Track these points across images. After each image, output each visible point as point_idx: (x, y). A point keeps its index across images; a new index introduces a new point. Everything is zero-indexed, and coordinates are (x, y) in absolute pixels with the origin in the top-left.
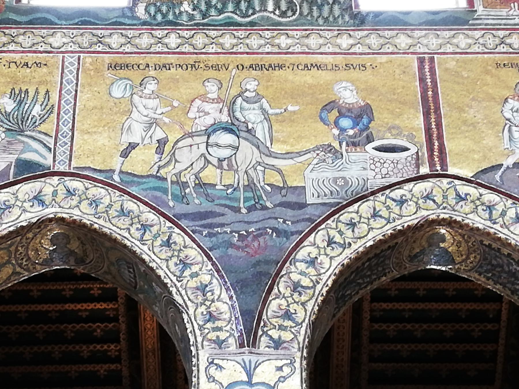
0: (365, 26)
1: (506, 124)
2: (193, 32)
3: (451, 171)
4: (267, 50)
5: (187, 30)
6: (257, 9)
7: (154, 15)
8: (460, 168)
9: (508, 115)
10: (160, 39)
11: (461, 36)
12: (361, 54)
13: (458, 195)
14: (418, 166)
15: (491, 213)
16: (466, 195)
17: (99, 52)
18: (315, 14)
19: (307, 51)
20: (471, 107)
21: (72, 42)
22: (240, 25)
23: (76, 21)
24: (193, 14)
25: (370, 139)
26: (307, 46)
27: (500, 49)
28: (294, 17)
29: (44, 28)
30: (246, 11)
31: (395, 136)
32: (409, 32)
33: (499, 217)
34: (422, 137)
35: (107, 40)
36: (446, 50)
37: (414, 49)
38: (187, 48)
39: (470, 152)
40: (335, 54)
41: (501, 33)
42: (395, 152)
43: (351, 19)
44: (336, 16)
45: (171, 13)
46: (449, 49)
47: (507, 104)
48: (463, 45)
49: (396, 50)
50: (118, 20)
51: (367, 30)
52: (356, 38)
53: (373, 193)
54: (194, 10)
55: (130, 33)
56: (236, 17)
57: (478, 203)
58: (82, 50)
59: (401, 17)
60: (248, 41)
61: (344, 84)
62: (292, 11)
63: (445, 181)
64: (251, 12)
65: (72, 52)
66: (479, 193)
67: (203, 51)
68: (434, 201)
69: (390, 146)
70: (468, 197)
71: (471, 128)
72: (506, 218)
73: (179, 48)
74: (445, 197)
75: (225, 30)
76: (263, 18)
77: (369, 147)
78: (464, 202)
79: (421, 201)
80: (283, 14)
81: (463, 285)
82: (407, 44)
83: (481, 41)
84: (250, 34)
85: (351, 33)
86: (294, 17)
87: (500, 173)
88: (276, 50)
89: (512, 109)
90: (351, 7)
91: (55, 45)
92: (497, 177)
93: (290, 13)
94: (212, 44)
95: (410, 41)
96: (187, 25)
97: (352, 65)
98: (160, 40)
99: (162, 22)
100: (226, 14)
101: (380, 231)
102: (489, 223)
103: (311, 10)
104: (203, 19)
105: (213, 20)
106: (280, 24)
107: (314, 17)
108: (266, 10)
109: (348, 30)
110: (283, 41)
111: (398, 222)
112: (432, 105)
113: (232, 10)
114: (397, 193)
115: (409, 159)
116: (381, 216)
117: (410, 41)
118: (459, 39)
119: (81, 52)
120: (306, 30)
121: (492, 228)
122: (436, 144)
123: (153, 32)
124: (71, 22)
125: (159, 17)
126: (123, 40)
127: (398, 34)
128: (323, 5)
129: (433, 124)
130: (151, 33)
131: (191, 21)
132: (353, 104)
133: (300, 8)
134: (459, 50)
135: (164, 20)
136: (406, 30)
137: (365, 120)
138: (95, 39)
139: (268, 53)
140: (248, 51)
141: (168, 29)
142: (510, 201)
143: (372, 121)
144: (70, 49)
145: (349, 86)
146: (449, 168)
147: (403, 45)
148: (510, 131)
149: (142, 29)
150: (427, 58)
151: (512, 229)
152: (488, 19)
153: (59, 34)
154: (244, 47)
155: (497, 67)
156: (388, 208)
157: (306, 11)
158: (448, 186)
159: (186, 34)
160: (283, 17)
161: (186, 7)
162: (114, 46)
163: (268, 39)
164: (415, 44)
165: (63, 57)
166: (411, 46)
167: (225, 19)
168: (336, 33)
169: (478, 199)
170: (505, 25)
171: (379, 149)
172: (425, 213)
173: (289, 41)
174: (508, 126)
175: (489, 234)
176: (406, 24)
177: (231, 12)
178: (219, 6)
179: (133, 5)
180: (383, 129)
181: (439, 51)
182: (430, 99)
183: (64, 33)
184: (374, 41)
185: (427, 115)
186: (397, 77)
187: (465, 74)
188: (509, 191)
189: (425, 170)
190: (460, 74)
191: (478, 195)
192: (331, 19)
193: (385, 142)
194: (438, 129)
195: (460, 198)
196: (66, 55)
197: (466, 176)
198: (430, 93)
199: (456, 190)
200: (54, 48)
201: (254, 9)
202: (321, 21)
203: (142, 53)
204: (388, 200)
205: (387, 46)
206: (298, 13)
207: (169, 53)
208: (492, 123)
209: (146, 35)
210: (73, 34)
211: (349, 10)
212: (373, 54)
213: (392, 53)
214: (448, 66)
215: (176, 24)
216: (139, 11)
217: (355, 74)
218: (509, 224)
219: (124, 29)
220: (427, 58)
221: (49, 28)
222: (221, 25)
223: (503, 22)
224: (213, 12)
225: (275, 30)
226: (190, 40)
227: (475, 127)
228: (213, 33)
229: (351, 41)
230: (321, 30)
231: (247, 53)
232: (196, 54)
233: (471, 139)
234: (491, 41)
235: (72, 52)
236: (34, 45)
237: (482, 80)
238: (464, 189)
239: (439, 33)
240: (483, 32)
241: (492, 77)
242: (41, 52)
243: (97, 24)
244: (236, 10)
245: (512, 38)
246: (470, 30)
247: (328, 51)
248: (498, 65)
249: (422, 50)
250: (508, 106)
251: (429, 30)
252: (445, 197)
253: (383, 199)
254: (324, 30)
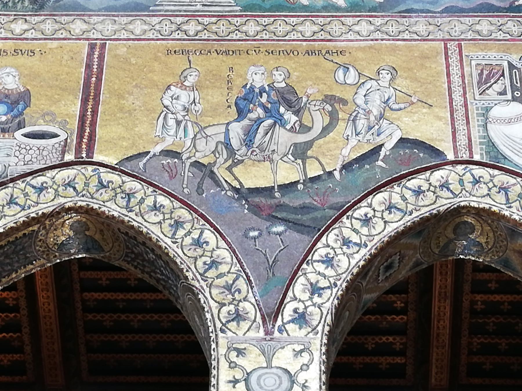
0: (43, 11)
1: (163, 111)
3: (97, 157)
8: (106, 156)
9: (167, 102)
11: (138, 22)
13: (100, 182)
14: (63, 153)
15: (129, 201)
16: (109, 182)
20: (131, 94)
25: (20, 126)
27: (175, 35)
31: (47, 123)
32: (86, 18)
33: (136, 205)
34: (75, 124)
36: (120, 36)
37: (88, 35)
39: (119, 139)
40: (6, 39)
41: (179, 20)
42: (44, 139)
43: (31, 5)
46: (124, 35)
47: (169, 91)
48: (138, 32)
49: (69, 36)
51: (45, 15)
52: (32, 23)
53: (13, 180)
57: (119, 190)
61: (8, 70)
63: (90, 168)
66: (122, 180)
68: (74, 188)
69: (39, 133)
70: (110, 184)
71: (127, 114)
72: (144, 206)
74: (87, 185)
77: (18, 134)
78: (105, 189)
79: (60, 189)
81: (114, 275)
82: (81, 30)
83: (157, 27)
85: (28, 18)
87: (145, 161)
89: (172, 97)
92: (141, 165)
95: (85, 27)
97: (21, 51)
101: (12, 218)
102: (124, 211)
109: (25, 15)
111: (33, 209)
112: (92, 91)
114: (38, 181)
115: (57, 146)
116: (16, 204)
117: (85, 27)
118: (136, 26)
121: (127, 216)
122: (88, 130)
127: (75, 19)
129: (90, 110)
132: (12, 90)
134: (132, 37)
137: (20, 107)
142: (151, 189)
143: (28, 106)
145: (13, 72)
146: (95, 155)
147: (77, 31)
148: (165, 118)
150: (98, 44)
151: (146, 217)
152: (170, 5)
155: (168, 54)
156: (26, 195)
158: (92, 174)
164: (89, 30)
166: (84, 32)
168: (12, 17)
169: (120, 187)
170: (185, 11)
171: (27, 136)
172: (62, 200)
174: (164, 113)
175: (123, 222)
176: (85, 9)
180: (38, 116)
181: (113, 37)
182: (93, 85)
184: (49, 26)
185: (85, 101)
186: (64, 62)
187: (133, 61)
188: (150, 179)
189: (69, 157)
190: (128, 60)
191: (121, 182)
193: (36, 128)
194: (93, 116)
195: (102, 185)
197: (111, 163)
198: (94, 79)
199: (99, 177)
204: (28, 187)
205: (61, 32)
208: (148, 111)
212: (45, 39)
213: (64, 39)
214: (118, 52)
217: (21, 60)
218: (145, 212)
220: (98, 44)
223: (184, 8)
227: (130, 114)
229: (26, 26)
233: (123, 126)
234: (167, 27)
237: (150, 66)
238: (107, 176)
239: (116, 18)
240: (162, 18)
241: (160, 64)
245: (189, 25)
248: (169, 52)
250: (170, 93)
251: (107, 15)
252: (87, 185)
253: (23, 186)
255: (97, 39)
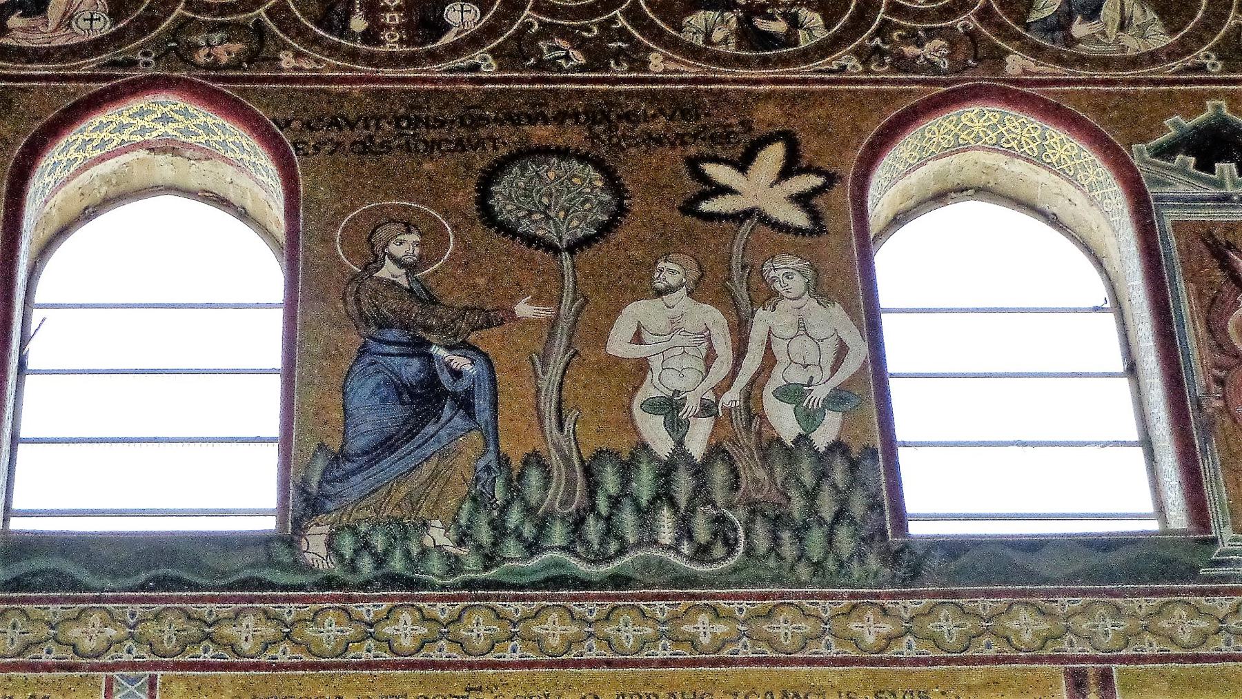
0: (923, 585)
2: (461, 604)
4: (661, 654)
5: (441, 599)
6: (631, 538)
7: (353, 561)
10: (371, 626)
11: (1180, 611)
12: (917, 662)
17: (206, 666)
18: (788, 551)
19: (770, 654)
21: (132, 636)
22: (586, 584)
23: (143, 577)
24: (456, 557)
26: (769, 642)
28: (732, 562)
29: (54, 601)
30: (601, 545)
32: (1039, 601)
35: (227, 630)
38: (443, 651)
40: (845, 662)
43: (886, 566)
44: (845, 557)
45: (398, 554)
50: (256, 573)
52: (902, 618)
54: (460, 543)
55: (289, 611)
56: (573, 561)
58: (158, 659)
59: (1017, 557)
60: (608, 630)
62: (726, 542)
64: (613, 547)
65: (133, 666)
67: (490, 657)
73: (423, 652)
75: (545, 598)
76: (647, 565)
80: (702, 553)
82: (1035, 634)
84: (614, 608)
85: (888, 603)
86: (732, 562)
88: (686, 653)
90: (883, 533)
91: (87, 645)
93: (719, 550)
94: (511, 639)
96: (443, 587)
98: (370, 630)
99: (376, 579)
100: (547, 555)
103: (776, 539)
104: (486, 568)
105: (511, 572)
106: (692, 580)
107: (782, 559)
108: (656, 542)
109: (878, 596)
110: (705, 629)
113: (564, 544)
117: (1044, 626)
119: (156, 666)
120: (765, 597)
123: (351, 606)
124: (129, 582)
125: (366, 565)
126: (269, 631)
128: (806, 527)
130: (345, 610)
131: (454, 575)
133: (747, 537)
134: (1175, 651)
135: (380, 573)
136: (1031, 594)
138: (193, 630)
139: (664, 663)
140: (610, 656)
141: (391, 599)
144: (126, 658)
147: (1027, 637)
149: (322, 599)
153: (96, 618)
154: (601, 648)
157: (762, 544)
159: (442, 611)
160: (702, 562)
161: (438, 536)
162: (246, 647)
163: (664, 623)
164: (1056, 632)
165: (110, 681)
167: (547, 567)
173: (721, 628)
176: (1032, 577)
177: (562, 549)
178: (528, 531)
179: (294, 533)
183: (110, 613)
184: (947, 625)
192: (831, 566)
196: (115, 674)
200: (83, 656)
201: (621, 538)
202: (803, 571)
203: (324, 667)
205: (985, 640)
206: (741, 549)
207: (396, 666)
209: (331, 617)
210: (133, 615)
211: (877, 538)
212: (949, 661)
213: (997, 660)
215: (411, 584)
216: (312, 549)
219: (274, 600)
220: (1091, 673)
221: (67, 600)
222: (534, 586)
224: (512, 548)
225: (679, 597)
226: (451, 627)
228: (515, 609)
229: (887, 628)
230: (806, 597)
231: (609, 663)
232: (471, 666)
235: (133, 666)
236: (27, 646)
239: (1119, 601)
242: (48, 668)
243: (197, 587)
244: (573, 542)
246: (1203, 593)
247: (825, 653)
249: (1076, 652)
254: (812, 596)
255: (1085, 659)
